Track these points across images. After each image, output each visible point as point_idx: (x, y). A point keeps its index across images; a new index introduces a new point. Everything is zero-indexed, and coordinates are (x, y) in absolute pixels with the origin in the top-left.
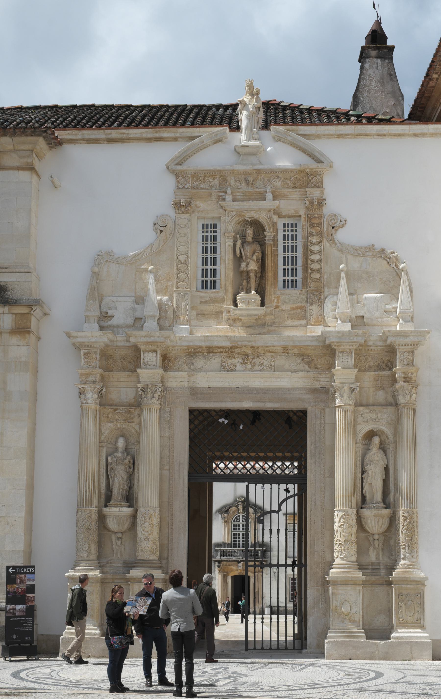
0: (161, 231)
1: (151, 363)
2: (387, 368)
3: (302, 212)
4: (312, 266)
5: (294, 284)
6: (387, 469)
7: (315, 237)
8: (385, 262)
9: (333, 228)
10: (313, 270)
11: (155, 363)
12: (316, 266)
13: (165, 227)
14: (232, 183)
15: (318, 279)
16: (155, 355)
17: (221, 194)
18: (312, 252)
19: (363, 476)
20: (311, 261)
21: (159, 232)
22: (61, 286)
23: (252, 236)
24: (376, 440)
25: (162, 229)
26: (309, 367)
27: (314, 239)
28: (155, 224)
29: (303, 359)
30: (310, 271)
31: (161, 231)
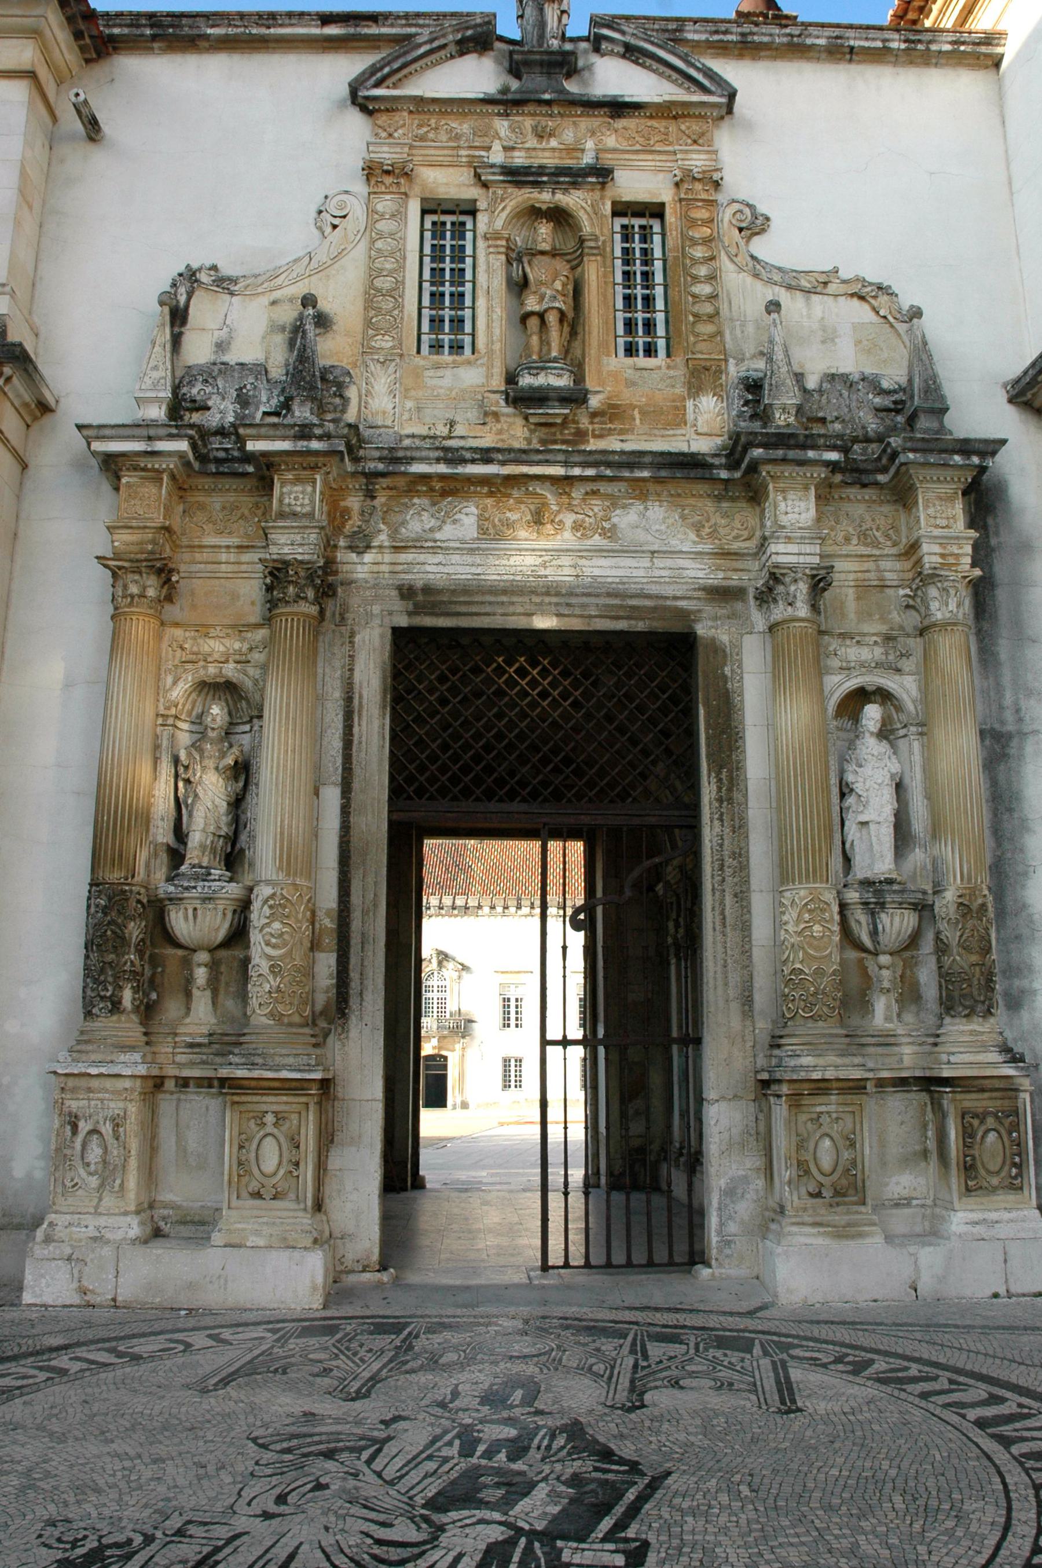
0: (335, 227)
1: (299, 509)
2: (889, 543)
3: (666, 194)
4: (696, 309)
5: (650, 351)
6: (899, 787)
7: (699, 248)
8: (866, 307)
9: (741, 230)
10: (695, 315)
11: (308, 509)
12: (708, 308)
13: (344, 217)
14: (502, 134)
15: (712, 336)
16: (309, 489)
17: (477, 153)
18: (695, 279)
19: (846, 804)
20: (694, 296)
21: (329, 229)
22: (102, 368)
23: (549, 240)
24: (872, 713)
25: (336, 221)
26: (698, 536)
27: (699, 252)
28: (320, 212)
29: (683, 517)
30: (691, 318)
31: (335, 227)
